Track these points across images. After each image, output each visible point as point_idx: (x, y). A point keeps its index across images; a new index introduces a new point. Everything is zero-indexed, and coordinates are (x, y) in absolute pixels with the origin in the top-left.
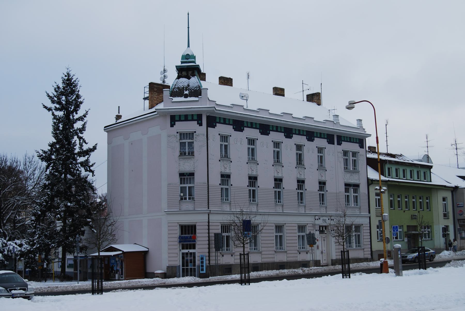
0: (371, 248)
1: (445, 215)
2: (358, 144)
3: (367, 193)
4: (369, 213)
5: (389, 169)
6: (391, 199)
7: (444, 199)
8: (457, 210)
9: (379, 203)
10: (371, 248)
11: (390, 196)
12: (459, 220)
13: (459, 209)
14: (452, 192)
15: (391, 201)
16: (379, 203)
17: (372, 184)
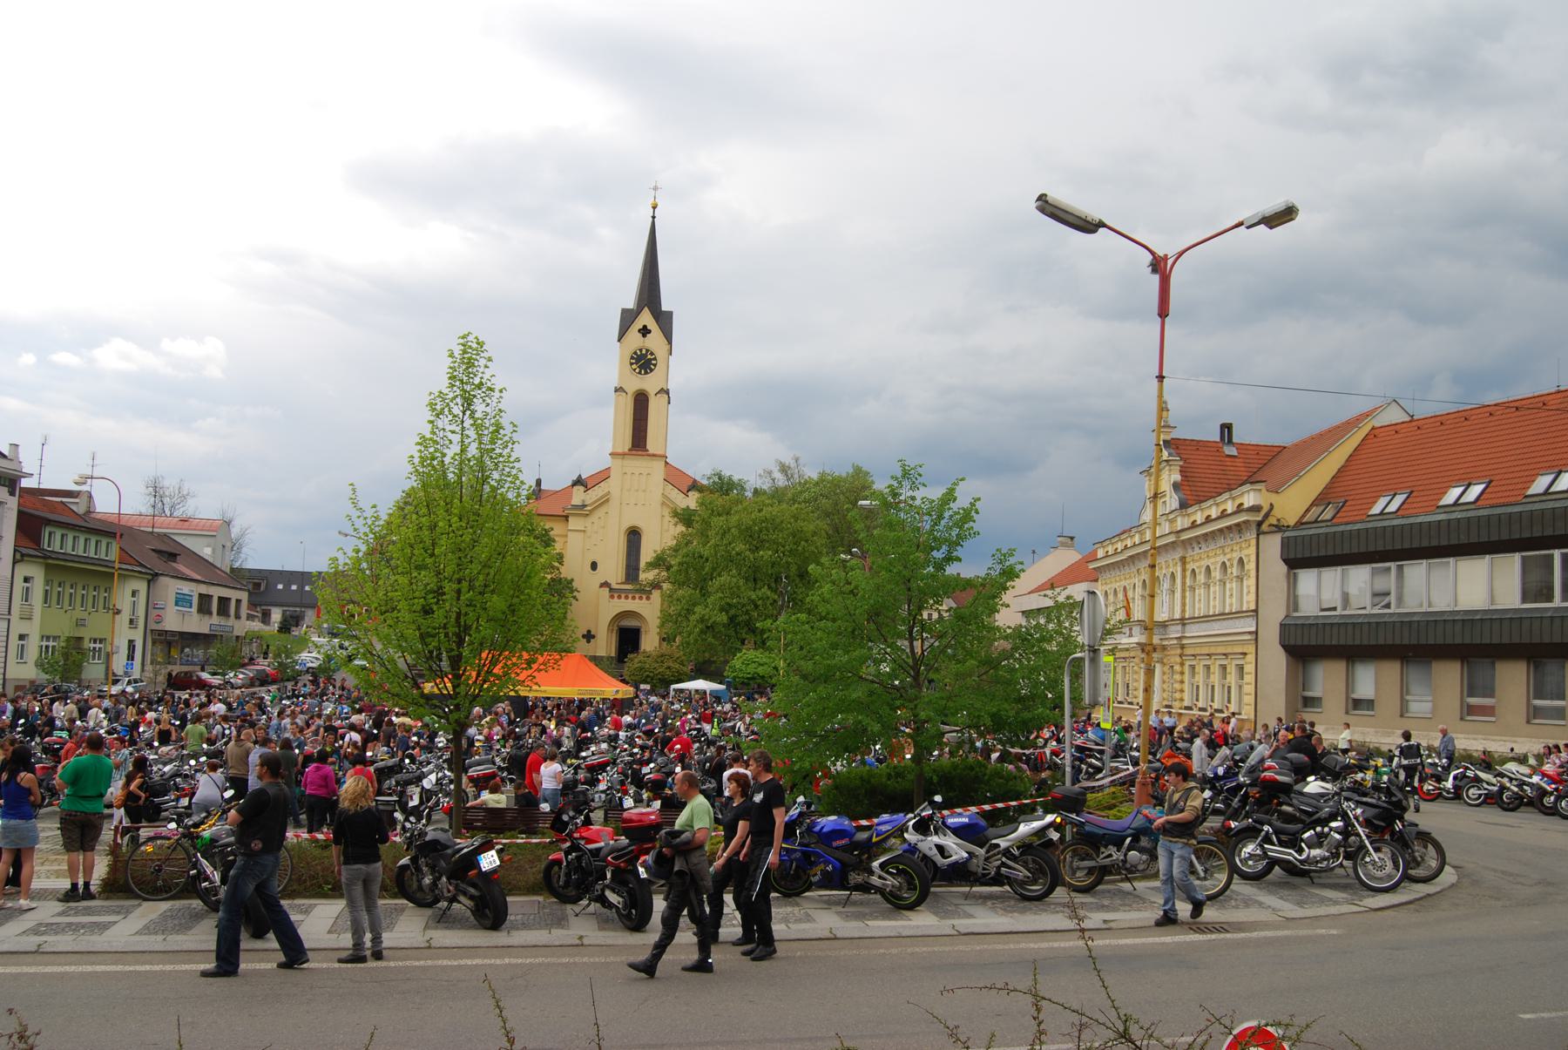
0: (4, 674)
1: (131, 621)
2: (6, 489)
3: (10, 576)
4: (9, 613)
5: (50, 534)
6: (48, 588)
7: (134, 594)
8: (153, 613)
9: (27, 594)
10: (4, 674)
11: (47, 582)
12: (152, 630)
13: (158, 612)
14: (149, 582)
15: (47, 591)
16: (27, 594)
17: (22, 561)
